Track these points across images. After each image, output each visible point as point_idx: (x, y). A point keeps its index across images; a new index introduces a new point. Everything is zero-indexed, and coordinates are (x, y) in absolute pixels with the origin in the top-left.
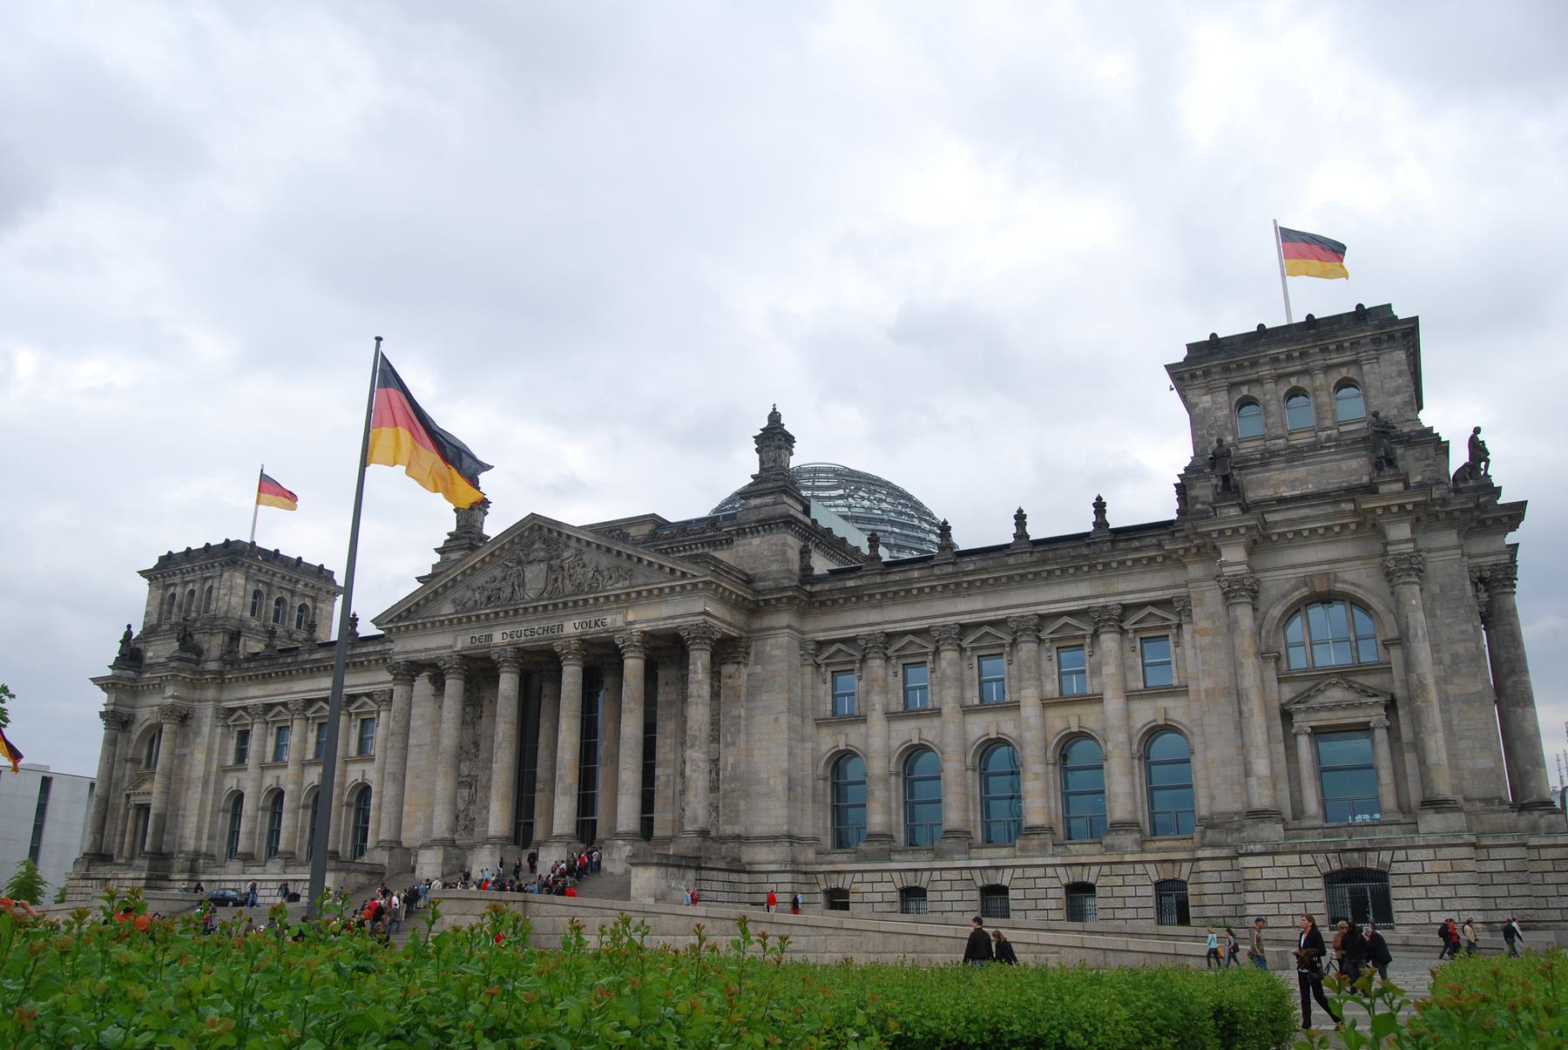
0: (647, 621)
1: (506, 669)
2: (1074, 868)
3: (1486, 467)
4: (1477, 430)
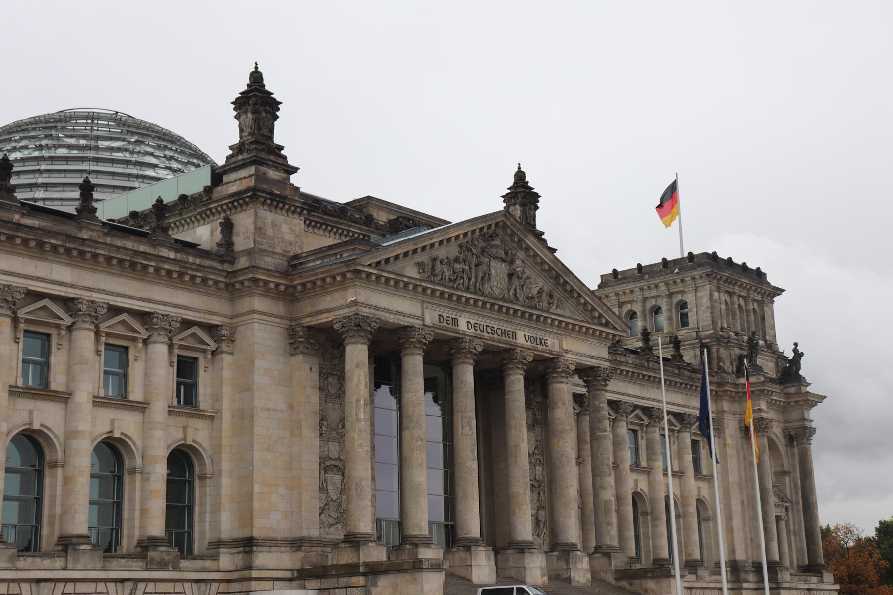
0: (577, 354)
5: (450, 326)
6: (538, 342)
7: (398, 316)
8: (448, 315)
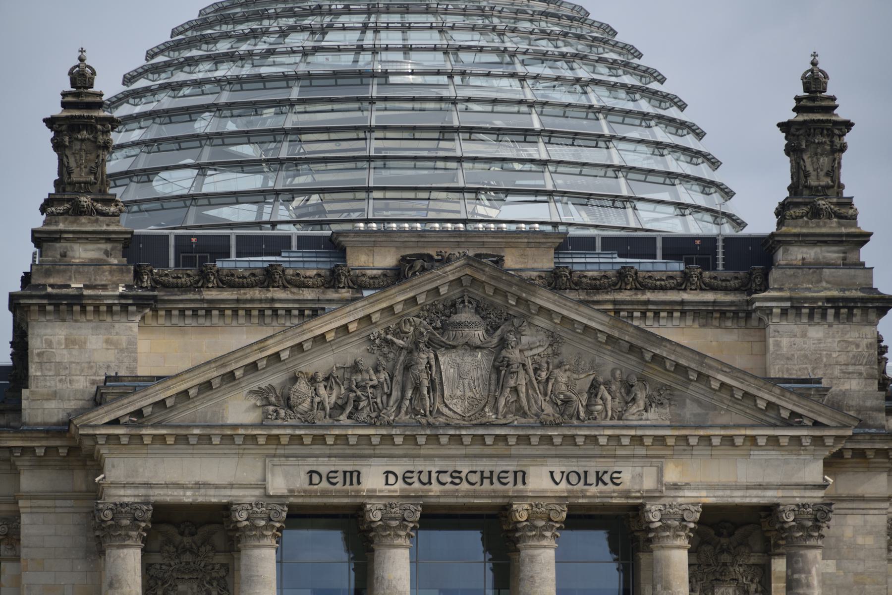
0: (710, 487)
1: (398, 541)
5: (339, 486)
6: (592, 479)
7: (202, 491)
8: (333, 469)
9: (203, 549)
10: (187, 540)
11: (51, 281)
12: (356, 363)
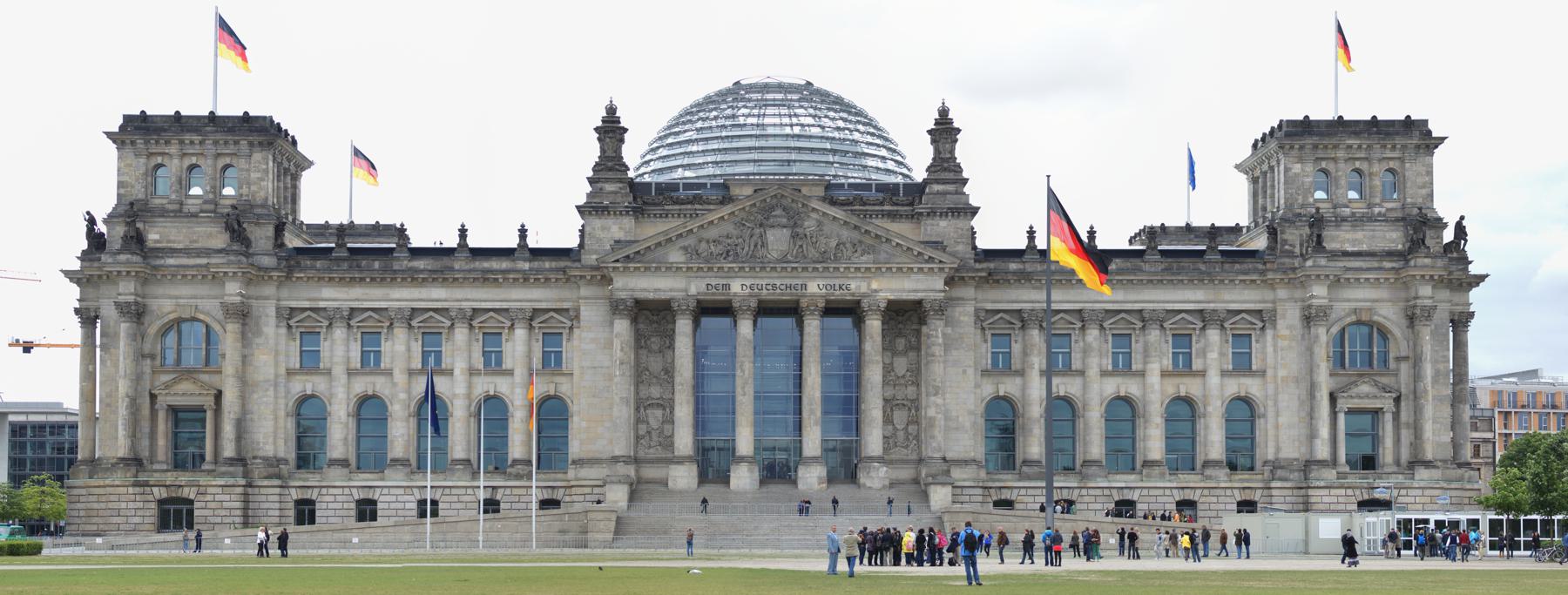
0: (892, 291)
1: (747, 316)
2: (1185, 490)
3: (1465, 245)
4: (1462, 218)
5: (720, 291)
6: (837, 288)
9: (662, 322)
10: (655, 318)
11: (595, 201)
12: (728, 234)
